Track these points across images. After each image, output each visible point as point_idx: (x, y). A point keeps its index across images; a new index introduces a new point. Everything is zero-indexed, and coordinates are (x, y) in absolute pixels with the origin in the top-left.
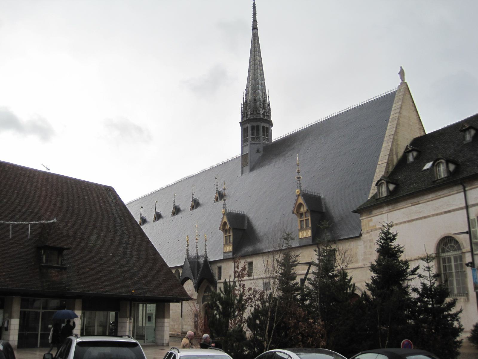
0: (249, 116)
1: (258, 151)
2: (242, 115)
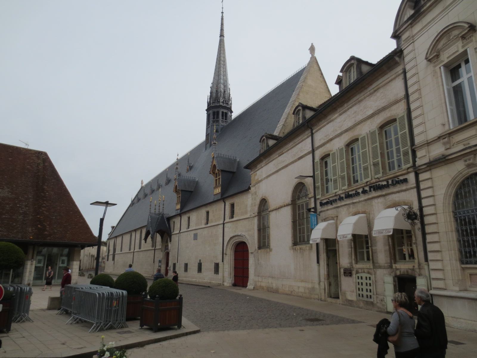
0: (211, 104)
2: (208, 104)
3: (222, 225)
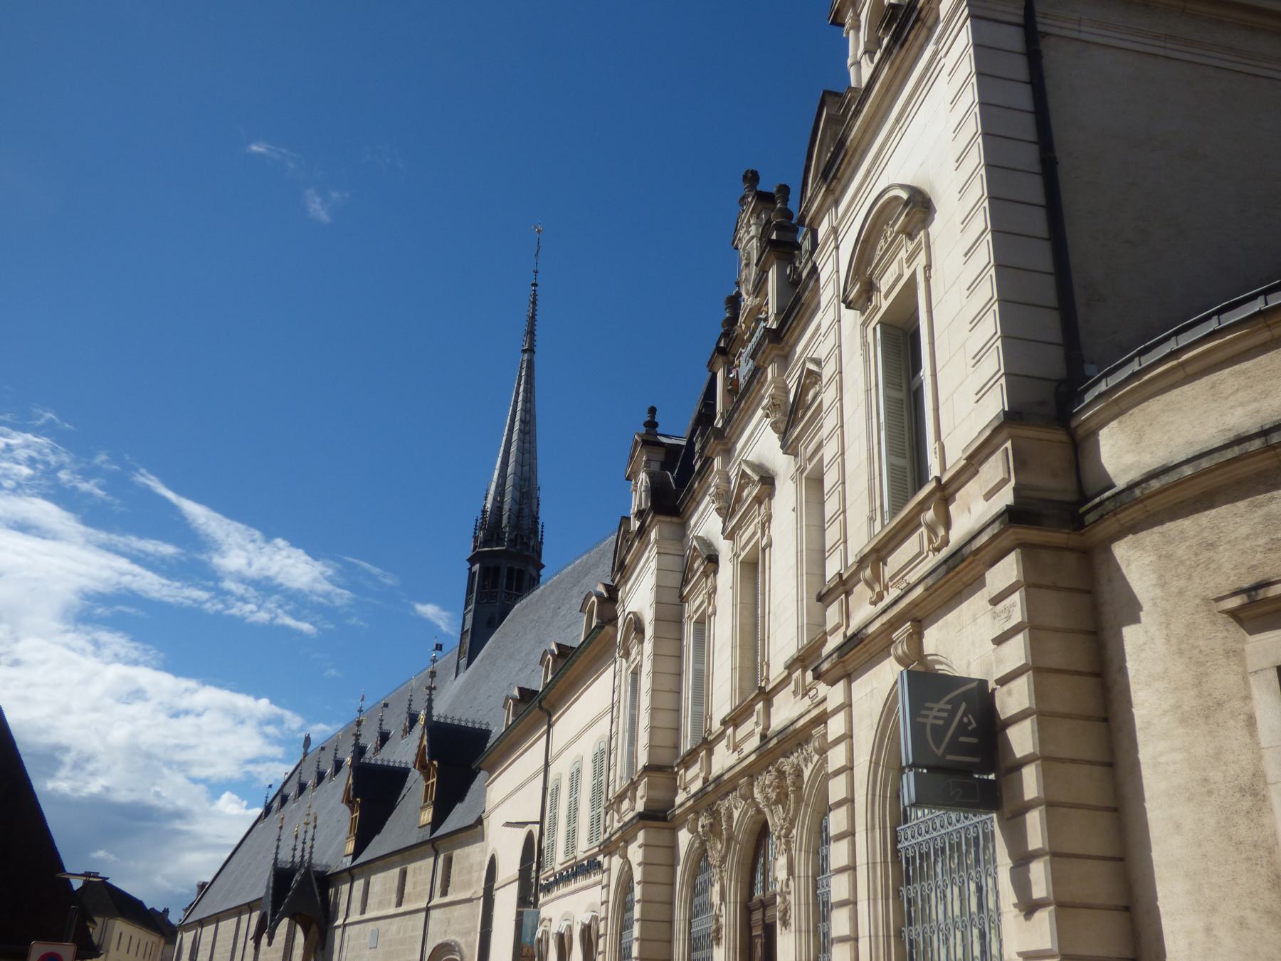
3: (424, 914)
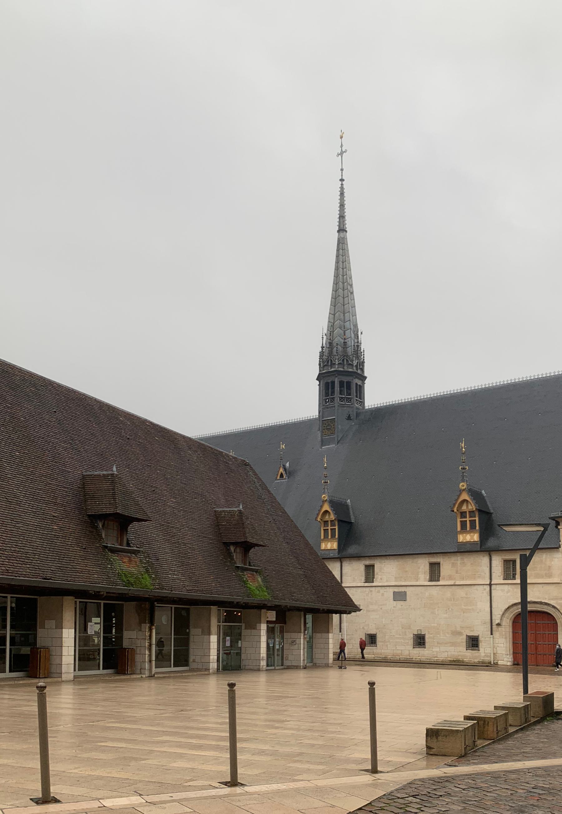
1: (349, 418)
